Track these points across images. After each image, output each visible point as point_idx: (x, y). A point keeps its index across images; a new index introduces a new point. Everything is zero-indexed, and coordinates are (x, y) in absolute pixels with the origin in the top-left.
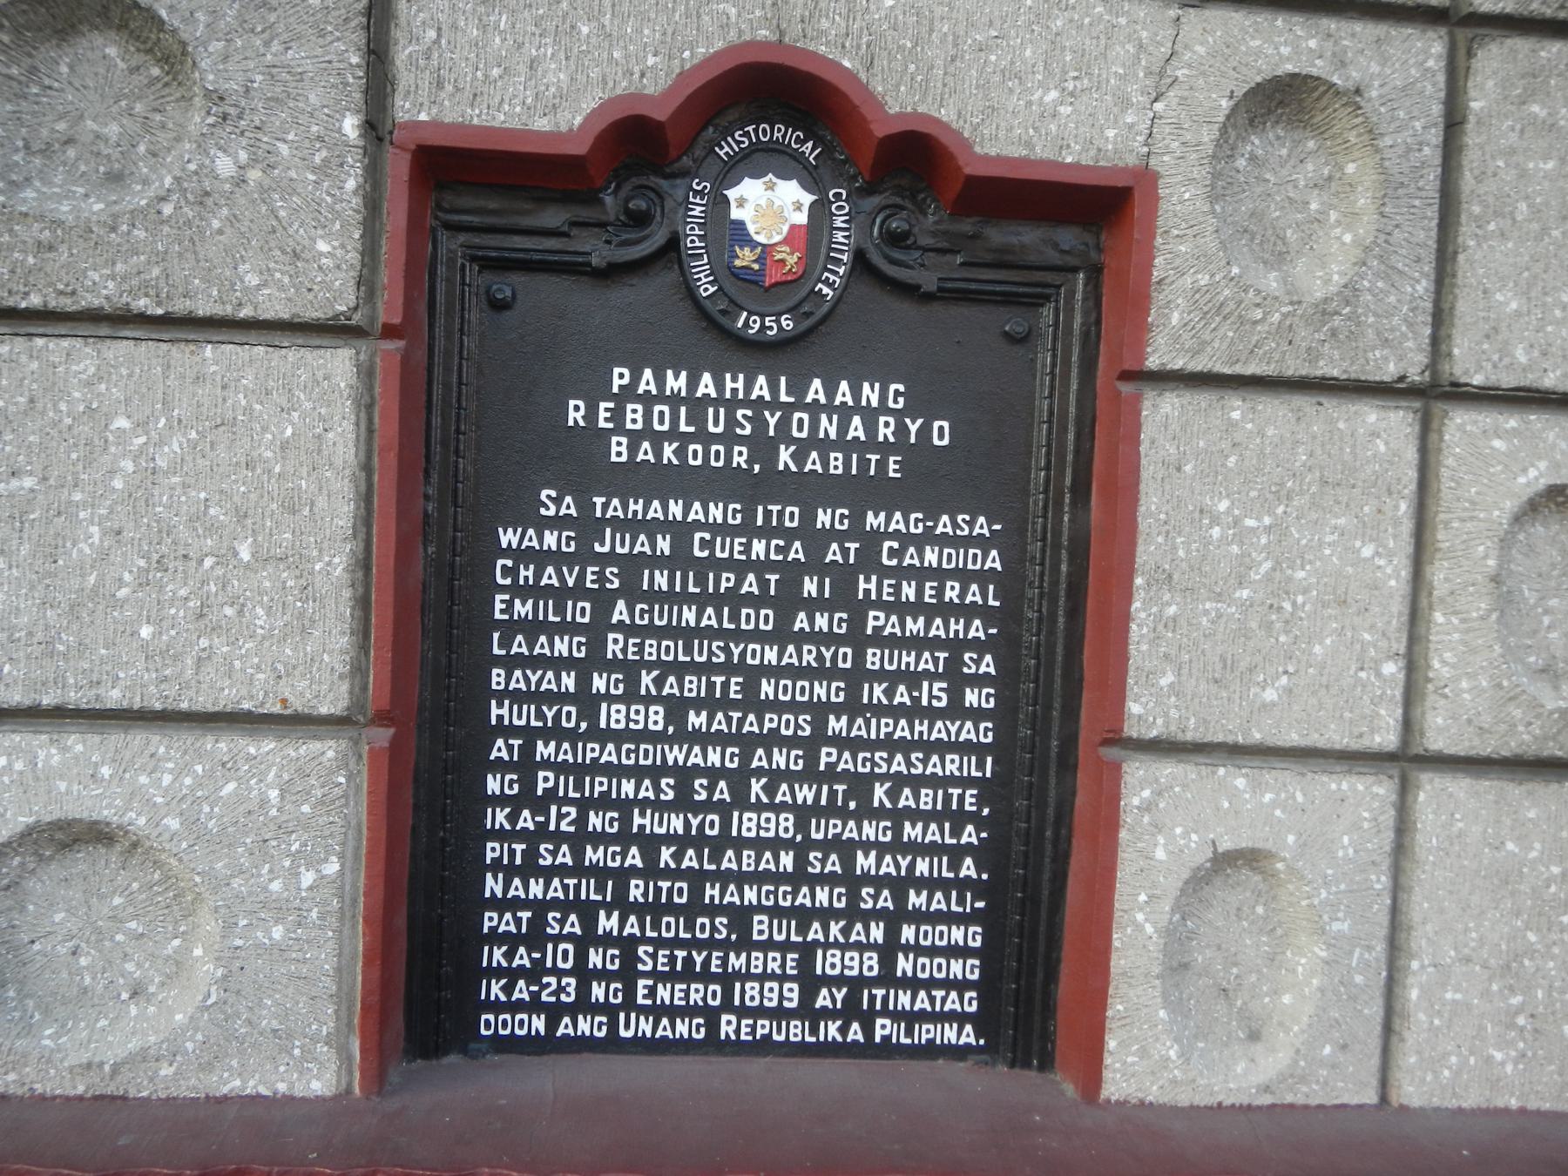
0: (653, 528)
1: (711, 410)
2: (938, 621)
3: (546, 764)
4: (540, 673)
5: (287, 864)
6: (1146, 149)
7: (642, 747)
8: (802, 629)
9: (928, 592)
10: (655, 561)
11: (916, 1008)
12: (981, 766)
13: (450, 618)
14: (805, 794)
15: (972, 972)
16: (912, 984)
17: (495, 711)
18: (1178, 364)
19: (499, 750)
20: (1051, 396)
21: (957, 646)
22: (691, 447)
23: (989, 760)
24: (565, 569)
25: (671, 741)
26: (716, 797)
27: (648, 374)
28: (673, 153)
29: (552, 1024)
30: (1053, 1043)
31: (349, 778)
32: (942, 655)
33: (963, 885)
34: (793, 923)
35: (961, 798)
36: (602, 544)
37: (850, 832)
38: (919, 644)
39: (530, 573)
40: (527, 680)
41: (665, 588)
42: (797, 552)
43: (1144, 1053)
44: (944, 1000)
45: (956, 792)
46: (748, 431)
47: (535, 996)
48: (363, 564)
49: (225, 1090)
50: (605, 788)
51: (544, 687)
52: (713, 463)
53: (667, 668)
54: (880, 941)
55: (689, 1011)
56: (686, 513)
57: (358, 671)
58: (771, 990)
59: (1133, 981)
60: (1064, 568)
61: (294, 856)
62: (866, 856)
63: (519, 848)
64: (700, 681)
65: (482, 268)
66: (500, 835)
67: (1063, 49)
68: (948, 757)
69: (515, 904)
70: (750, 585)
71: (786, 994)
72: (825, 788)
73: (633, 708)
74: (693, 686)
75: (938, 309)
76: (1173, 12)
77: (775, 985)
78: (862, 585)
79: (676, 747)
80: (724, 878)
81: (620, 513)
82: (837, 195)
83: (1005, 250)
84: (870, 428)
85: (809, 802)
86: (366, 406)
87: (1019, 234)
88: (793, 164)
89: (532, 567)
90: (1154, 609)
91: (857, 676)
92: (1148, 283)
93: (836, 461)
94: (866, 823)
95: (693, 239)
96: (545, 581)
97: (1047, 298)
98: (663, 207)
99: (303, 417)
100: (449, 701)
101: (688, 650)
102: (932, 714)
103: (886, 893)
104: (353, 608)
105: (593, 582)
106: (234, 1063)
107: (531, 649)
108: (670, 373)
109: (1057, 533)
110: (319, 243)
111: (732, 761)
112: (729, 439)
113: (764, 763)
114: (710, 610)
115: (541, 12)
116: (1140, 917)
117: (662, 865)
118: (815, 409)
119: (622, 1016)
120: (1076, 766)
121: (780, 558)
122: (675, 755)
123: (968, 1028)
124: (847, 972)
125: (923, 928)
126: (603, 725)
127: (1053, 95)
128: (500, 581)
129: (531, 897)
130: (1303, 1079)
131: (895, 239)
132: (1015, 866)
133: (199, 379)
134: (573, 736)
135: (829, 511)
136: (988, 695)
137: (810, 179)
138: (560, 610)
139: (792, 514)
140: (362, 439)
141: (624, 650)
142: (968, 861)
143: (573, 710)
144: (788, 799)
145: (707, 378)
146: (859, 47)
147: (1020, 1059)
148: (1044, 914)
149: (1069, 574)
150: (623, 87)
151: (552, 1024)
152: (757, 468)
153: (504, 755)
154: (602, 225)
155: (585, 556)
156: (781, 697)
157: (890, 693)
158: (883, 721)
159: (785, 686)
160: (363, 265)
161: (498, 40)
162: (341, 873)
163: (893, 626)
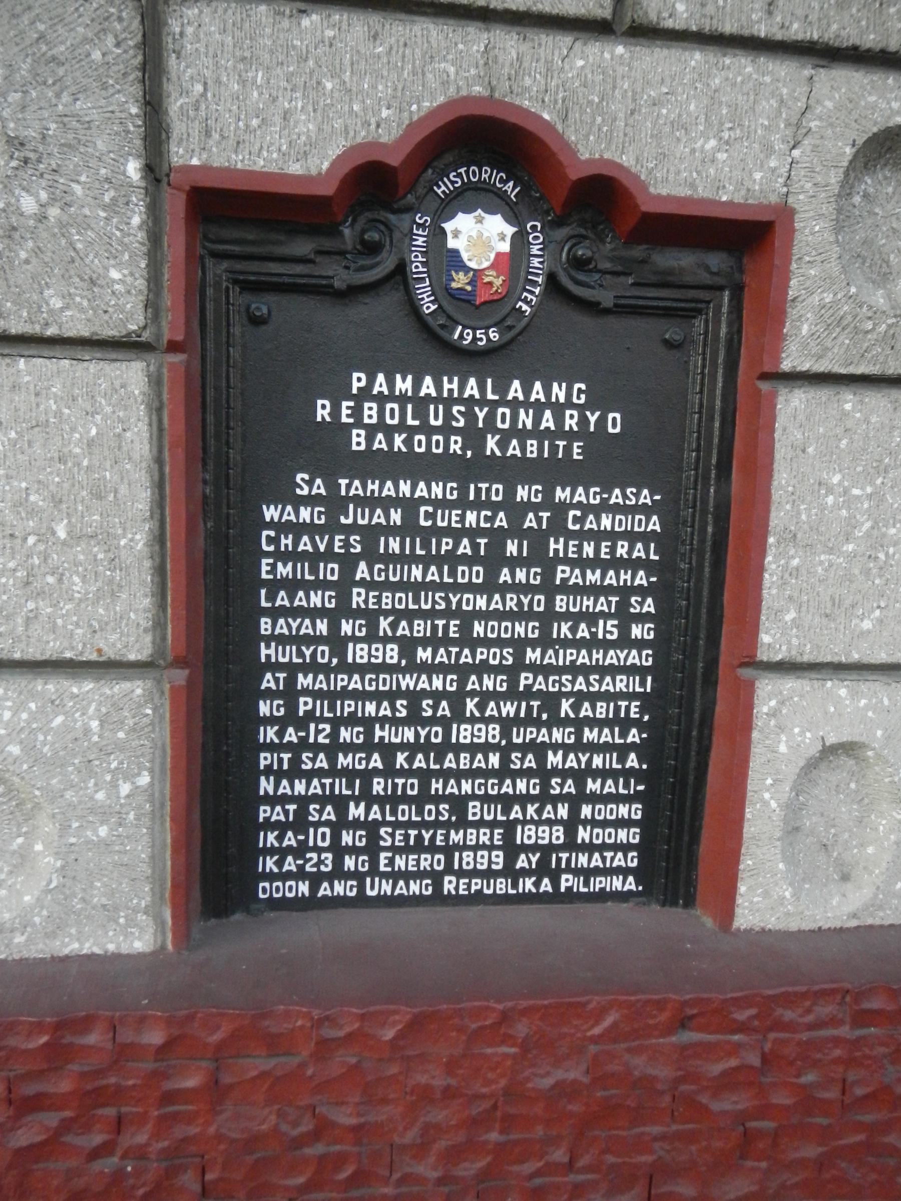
0: (387, 504)
1: (432, 407)
2: (611, 573)
3: (306, 692)
4: (299, 620)
5: (108, 778)
6: (785, 189)
7: (381, 676)
8: (505, 582)
9: (604, 550)
10: (389, 530)
11: (592, 866)
12: (643, 683)
13: (227, 579)
14: (508, 709)
15: (634, 838)
16: (589, 848)
17: (264, 652)
18: (805, 367)
19: (268, 681)
20: (701, 392)
21: (625, 592)
22: (417, 438)
23: (649, 679)
24: (317, 538)
25: (404, 671)
26: (440, 713)
27: (381, 378)
28: (401, 192)
29: (314, 888)
30: (695, 887)
31: (155, 710)
32: (614, 599)
33: (628, 773)
34: (499, 807)
35: (628, 708)
36: (347, 517)
37: (543, 736)
38: (596, 591)
39: (289, 541)
40: (289, 627)
41: (397, 551)
42: (501, 520)
43: (766, 894)
44: (613, 859)
45: (623, 704)
46: (462, 423)
47: (301, 868)
48: (159, 539)
49: (66, 951)
50: (352, 709)
51: (303, 631)
52: (434, 450)
53: (399, 615)
54: (565, 817)
55: (420, 875)
56: (413, 491)
57: (158, 625)
58: (482, 857)
59: (760, 843)
60: (710, 529)
61: (113, 772)
62: (555, 754)
63: (286, 756)
64: (426, 624)
65: (243, 289)
66: (271, 747)
67: (721, 103)
68: (618, 678)
69: (284, 800)
70: (465, 548)
71: (494, 859)
72: (524, 704)
73: (374, 646)
74: (420, 628)
75: (611, 321)
76: (807, 72)
77: (486, 853)
78: (552, 546)
79: (408, 676)
80: (445, 775)
81: (361, 492)
82: (534, 228)
83: (670, 272)
84: (559, 419)
85: (512, 715)
86: (156, 409)
87: (680, 259)
88: (499, 201)
89: (290, 536)
90: (782, 562)
91: (549, 617)
92: (785, 301)
93: (532, 446)
94: (555, 730)
95: (417, 266)
96: (301, 548)
97: (699, 311)
98: (391, 237)
99: (105, 418)
100: (227, 644)
101: (416, 600)
102: (606, 645)
103: (570, 782)
104: (152, 575)
105: (340, 547)
106: (73, 931)
107: (292, 601)
108: (398, 377)
109: (704, 502)
110: (111, 269)
111: (451, 685)
112: (447, 430)
113: (477, 687)
114: (433, 568)
115: (291, 69)
116: (767, 796)
117: (398, 767)
118: (515, 405)
119: (368, 880)
120: (716, 683)
121: (488, 525)
122: (407, 682)
123: (631, 879)
124: (540, 842)
125: (597, 807)
126: (350, 660)
127: (713, 143)
128: (265, 548)
129: (296, 793)
130: (881, 908)
131: (579, 264)
132: (668, 758)
133: (14, 387)
134: (326, 669)
135: (527, 487)
136: (649, 629)
137: (511, 214)
138: (314, 570)
139: (497, 490)
140: (155, 438)
141: (366, 601)
142: (633, 756)
143: (326, 649)
144: (495, 713)
145: (428, 380)
146: (556, 102)
147: (670, 900)
148: (690, 794)
149: (714, 534)
150: (362, 136)
151: (314, 888)
152: (469, 453)
153: (272, 685)
154: (342, 253)
155: (332, 527)
156: (489, 635)
157: (574, 629)
158: (569, 651)
159: (493, 627)
160: (149, 290)
161: (255, 94)
162: (151, 784)
163: (577, 577)
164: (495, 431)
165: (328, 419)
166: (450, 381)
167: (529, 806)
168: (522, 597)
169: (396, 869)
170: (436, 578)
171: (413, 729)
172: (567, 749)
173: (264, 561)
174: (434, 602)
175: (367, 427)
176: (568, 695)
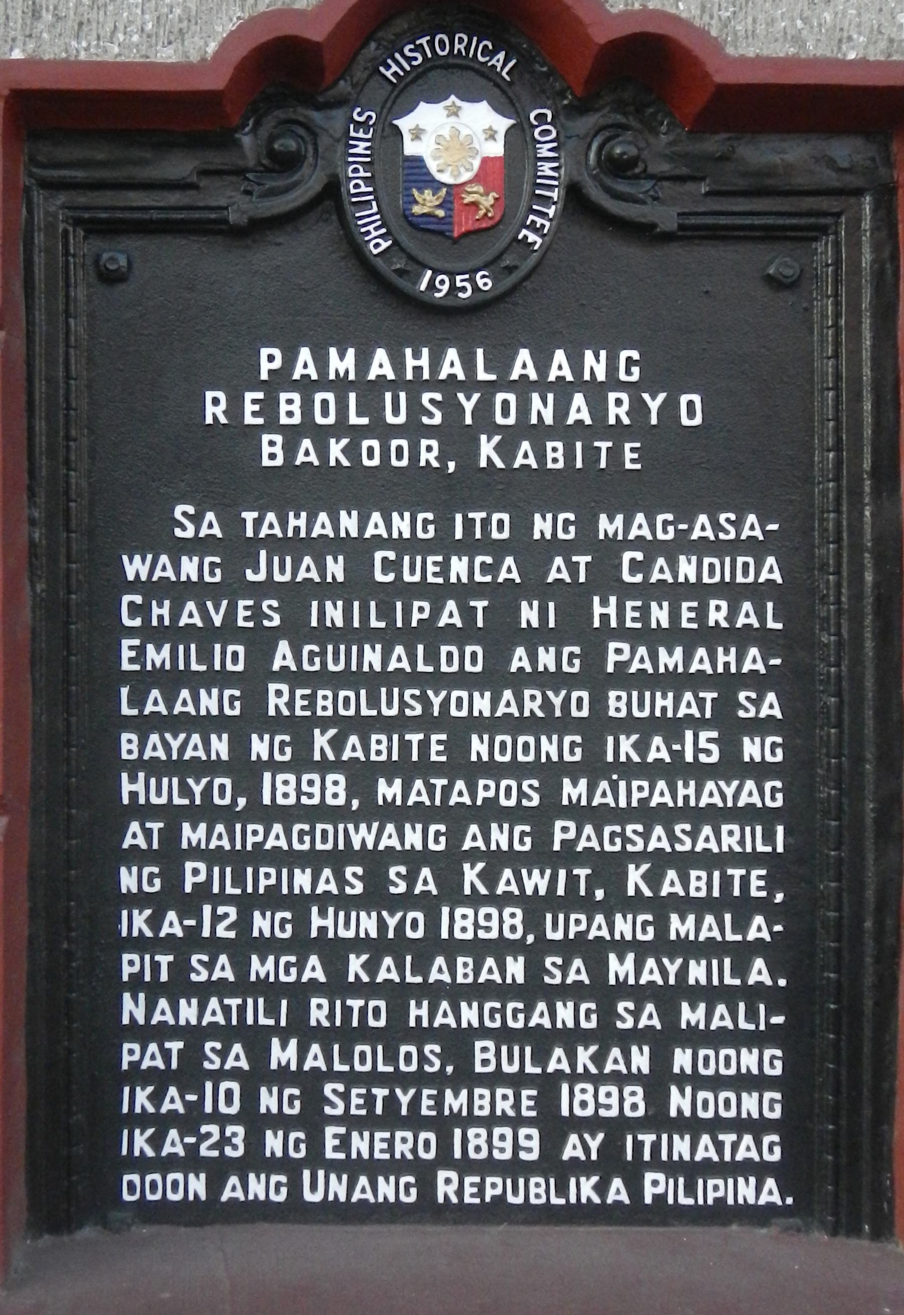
0: (319, 548)
1: (388, 396)
2: (701, 652)
7: (319, 827)
9: (686, 615)
10: (326, 590)
14: (536, 881)
24: (209, 604)
25: (356, 818)
26: (419, 888)
27: (305, 354)
32: (709, 696)
36: (256, 571)
37: (598, 929)
38: (676, 682)
39: (165, 611)
41: (339, 623)
42: (510, 569)
46: (437, 420)
51: (189, 754)
55: (395, 1167)
64: (390, 740)
70: (450, 615)
72: (562, 874)
73: (305, 778)
74: (381, 747)
78: (598, 610)
80: (433, 993)
81: (277, 531)
84: (598, 407)
85: (542, 892)
89: (167, 603)
91: (597, 727)
96: (184, 621)
101: (373, 702)
102: (700, 773)
107: (170, 706)
108: (333, 351)
112: (414, 430)
114: (399, 650)
118: (523, 387)
119: (306, 1174)
122: (362, 836)
135: (549, 516)
138: (205, 656)
139: (501, 523)
141: (291, 705)
152: (452, 466)
155: (233, 587)
157: (642, 747)
163: (642, 660)
164: (494, 429)
165: (223, 420)
166: (417, 355)
167: (580, 1049)
168: (550, 694)
169: (354, 1155)
170: (405, 665)
171: (374, 914)
172: (641, 950)
173: (126, 643)
174: (403, 704)
175: (285, 430)
176: (638, 858)
